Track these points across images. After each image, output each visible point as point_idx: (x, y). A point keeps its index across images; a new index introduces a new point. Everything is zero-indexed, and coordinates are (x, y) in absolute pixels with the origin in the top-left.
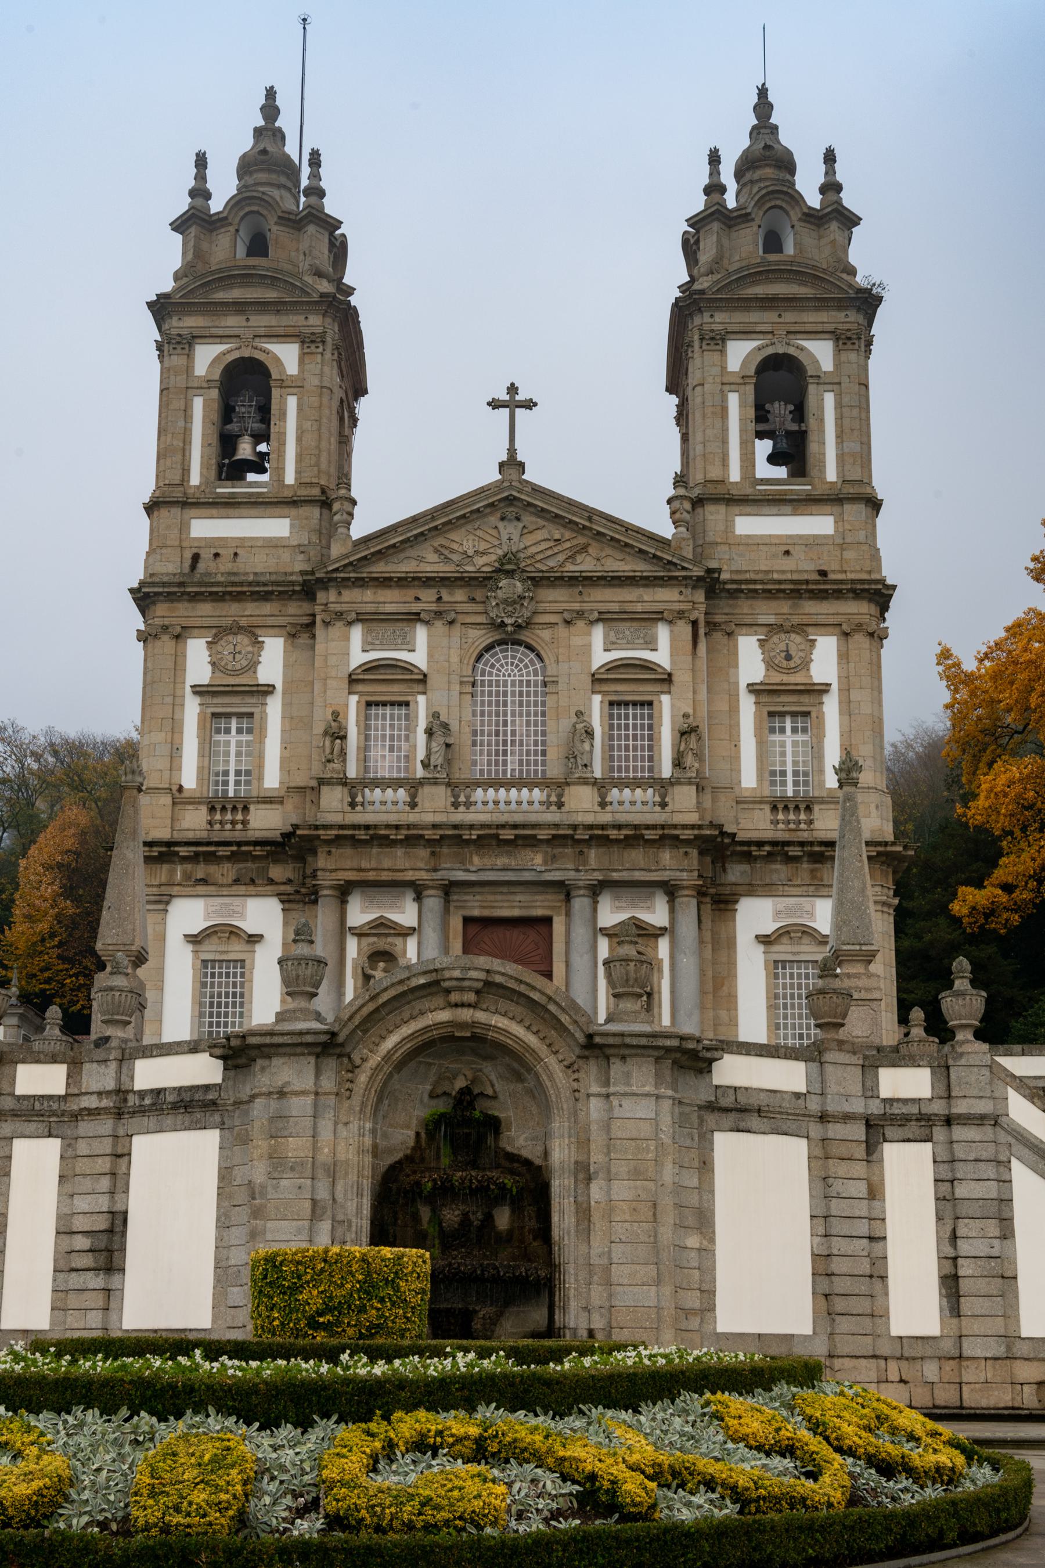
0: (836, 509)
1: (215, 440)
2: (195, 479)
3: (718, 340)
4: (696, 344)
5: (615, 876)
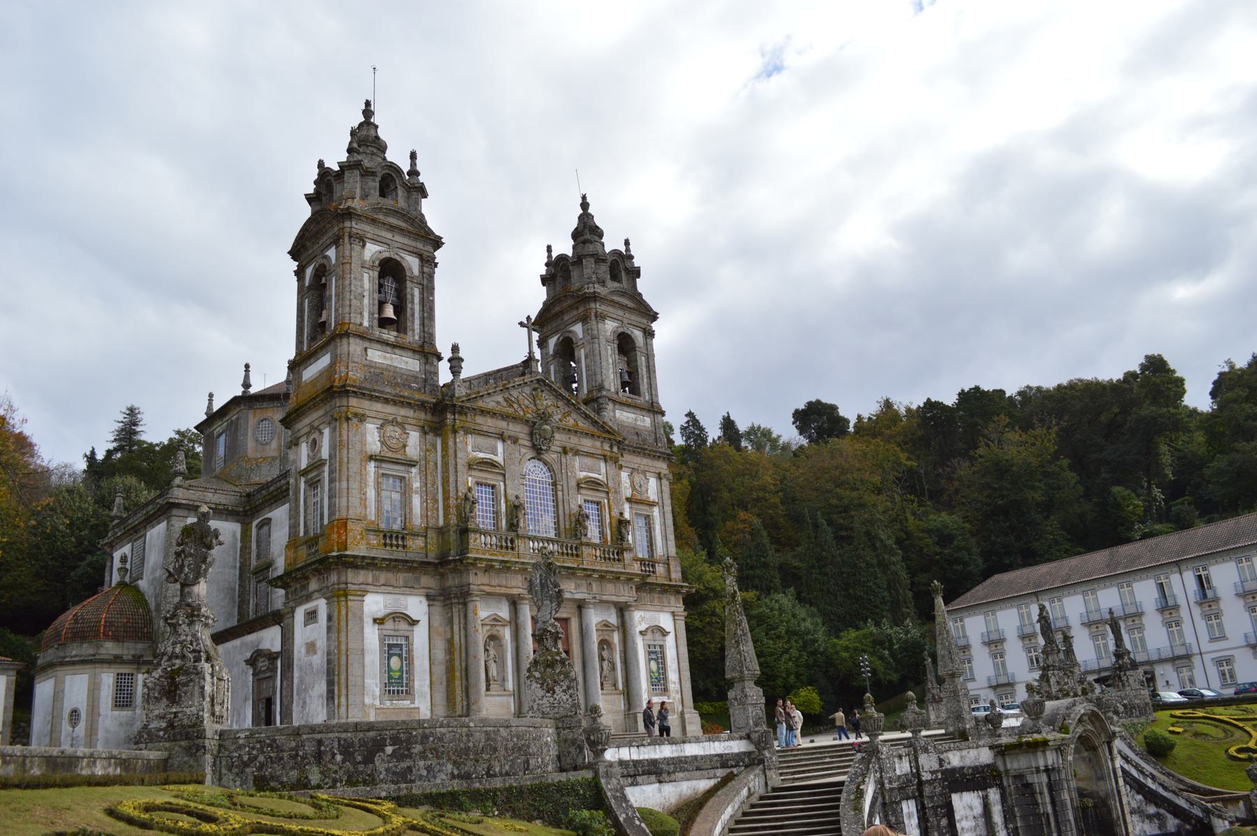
0: (651, 415)
2: (366, 324)
3: (601, 317)
4: (593, 318)
5: (604, 598)
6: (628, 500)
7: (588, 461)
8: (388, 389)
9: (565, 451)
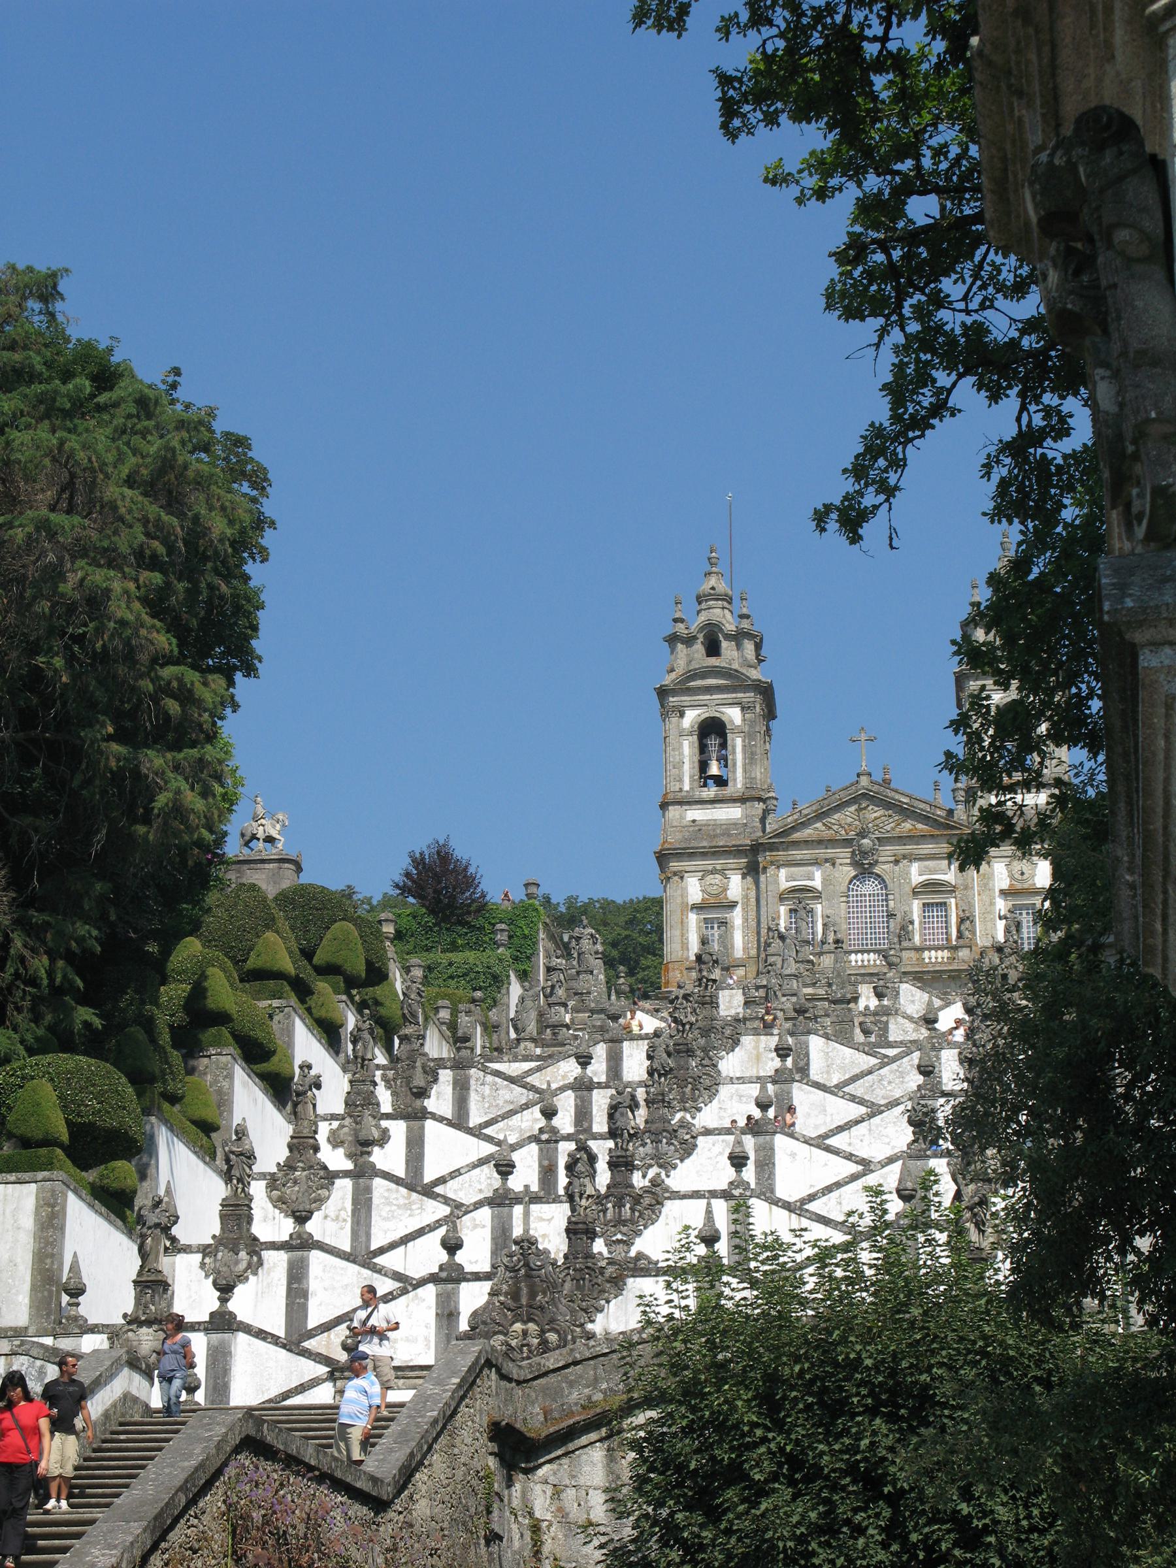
1: (697, 765)
2: (687, 787)
6: (1003, 893)
7: (931, 864)
8: (705, 844)
9: (897, 862)
